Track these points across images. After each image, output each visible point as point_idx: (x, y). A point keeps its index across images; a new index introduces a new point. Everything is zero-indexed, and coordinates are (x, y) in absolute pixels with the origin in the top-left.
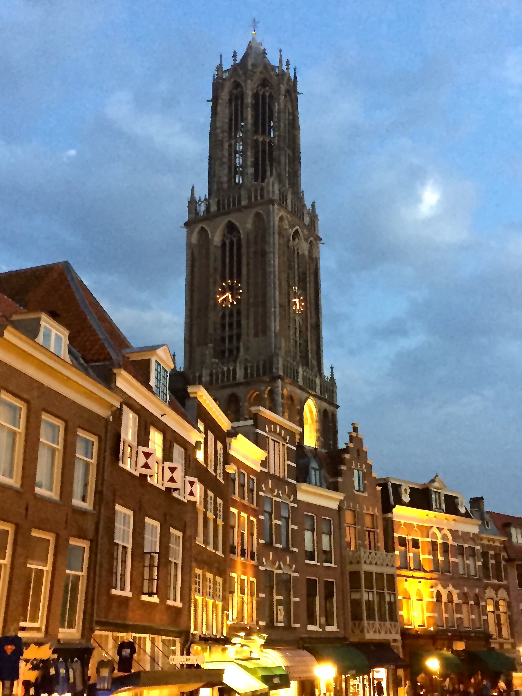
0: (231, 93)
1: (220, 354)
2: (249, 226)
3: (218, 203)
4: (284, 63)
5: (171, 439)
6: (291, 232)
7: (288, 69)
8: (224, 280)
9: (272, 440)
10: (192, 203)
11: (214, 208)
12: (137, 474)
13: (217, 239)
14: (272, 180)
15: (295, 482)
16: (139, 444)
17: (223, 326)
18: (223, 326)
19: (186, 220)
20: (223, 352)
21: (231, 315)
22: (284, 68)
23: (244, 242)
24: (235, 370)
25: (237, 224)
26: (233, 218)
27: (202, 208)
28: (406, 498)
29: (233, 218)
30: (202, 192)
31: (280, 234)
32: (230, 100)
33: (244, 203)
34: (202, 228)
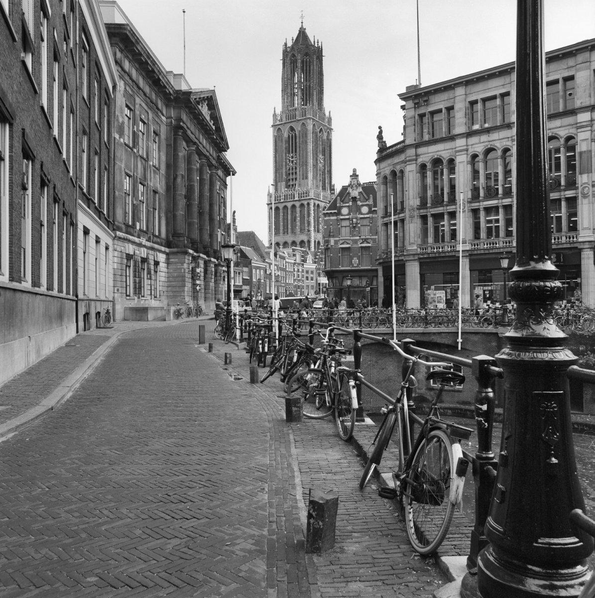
0: (291, 59)
1: (288, 186)
2: (299, 129)
6: (319, 130)
8: (289, 153)
10: (275, 115)
11: (284, 119)
13: (286, 135)
19: (272, 124)
20: (289, 186)
21: (292, 169)
22: (316, 45)
23: (298, 135)
26: (291, 124)
29: (291, 124)
30: (279, 110)
32: (291, 63)
34: (279, 128)
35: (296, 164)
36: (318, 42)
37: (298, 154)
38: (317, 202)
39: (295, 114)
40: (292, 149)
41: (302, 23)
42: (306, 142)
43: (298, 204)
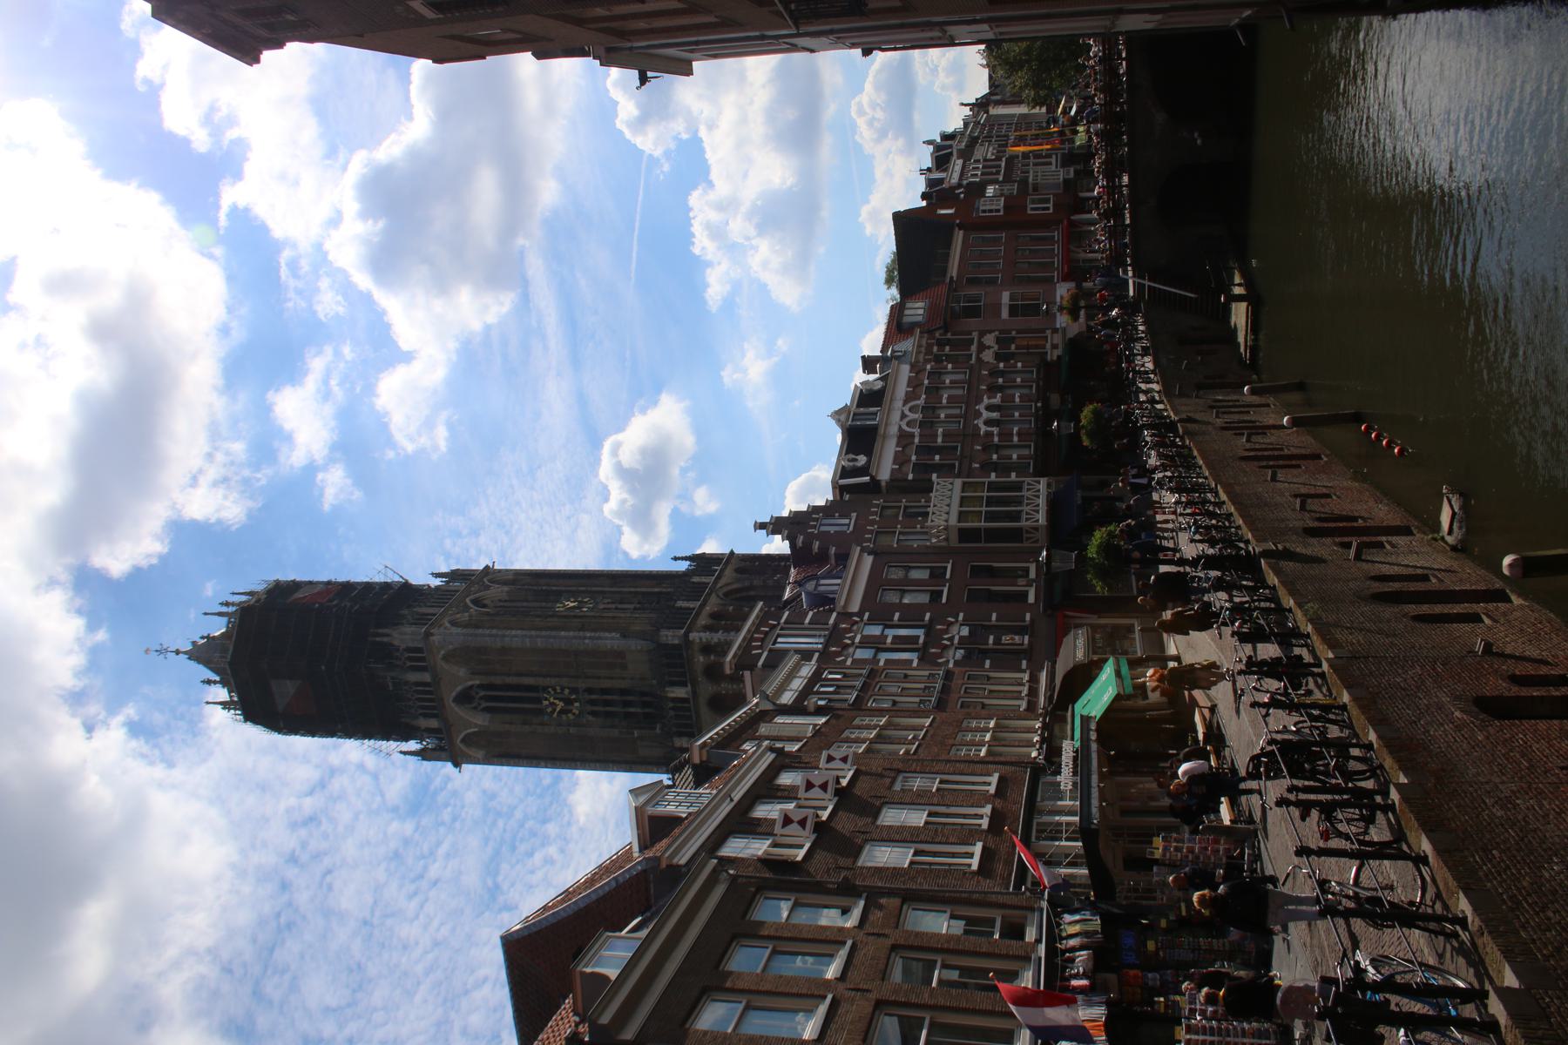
2: (462, 672)
3: (425, 716)
4: (224, 609)
5: (766, 789)
7: (233, 604)
8: (541, 712)
9: (775, 642)
12: (813, 837)
13: (479, 720)
14: (395, 634)
15: (834, 615)
16: (771, 834)
17: (608, 715)
18: (608, 715)
19: (449, 764)
21: (592, 702)
22: (231, 609)
23: (485, 680)
24: (674, 700)
25: (459, 688)
27: (429, 743)
28: (862, 460)
29: (449, 696)
31: (477, 627)
33: (427, 677)
34: (463, 741)
35: (574, 690)
36: (227, 604)
37: (540, 681)
38: (703, 620)
39: (418, 684)
40: (529, 700)
41: (178, 652)
42: (504, 651)
43: (707, 689)
